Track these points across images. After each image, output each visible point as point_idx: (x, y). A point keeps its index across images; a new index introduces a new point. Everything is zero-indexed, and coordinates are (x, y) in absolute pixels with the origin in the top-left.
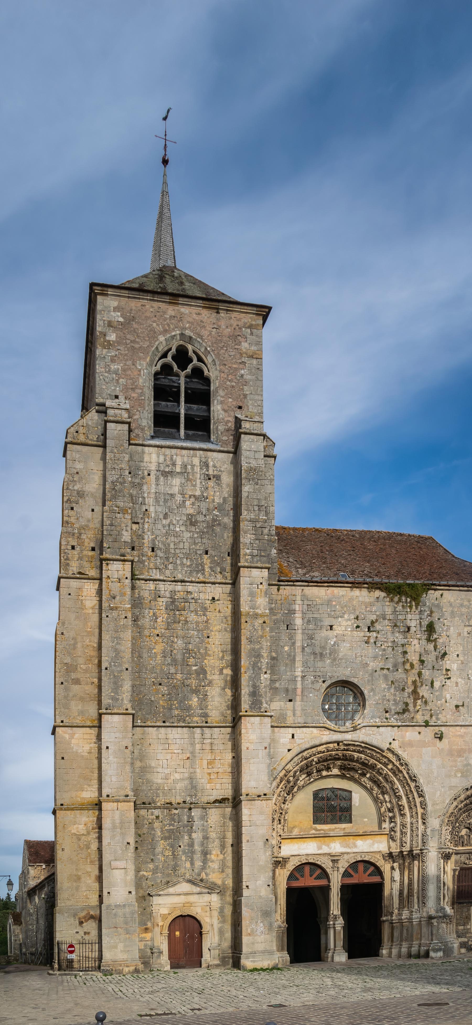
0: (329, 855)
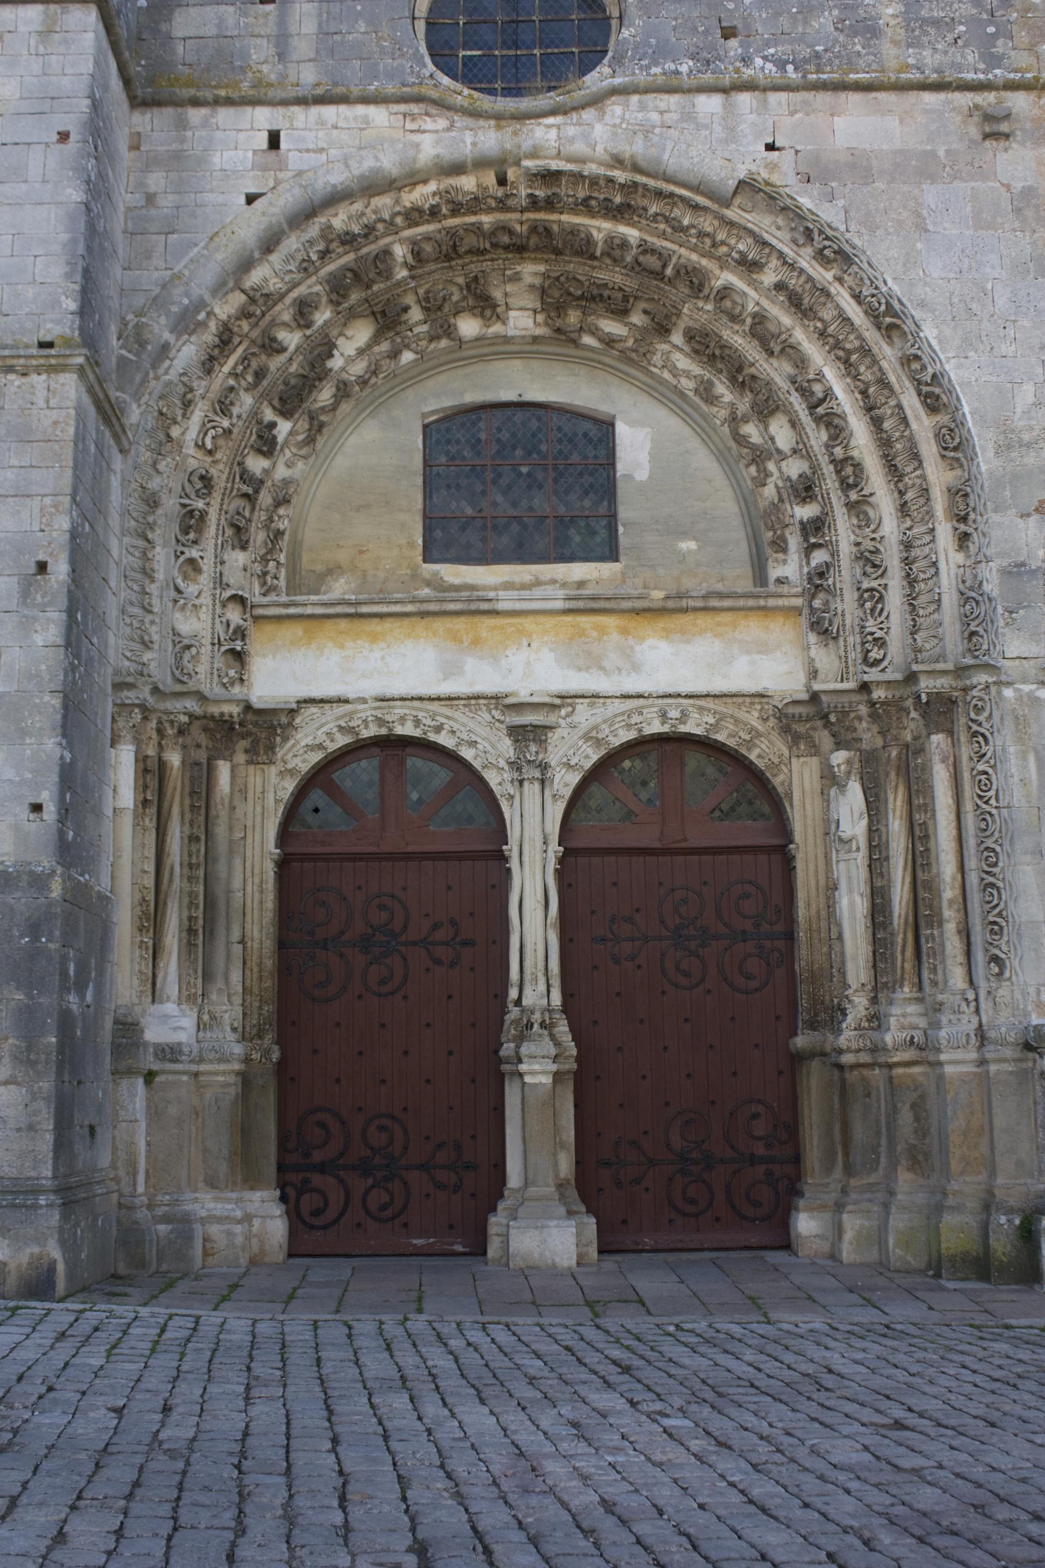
0: (496, 700)
